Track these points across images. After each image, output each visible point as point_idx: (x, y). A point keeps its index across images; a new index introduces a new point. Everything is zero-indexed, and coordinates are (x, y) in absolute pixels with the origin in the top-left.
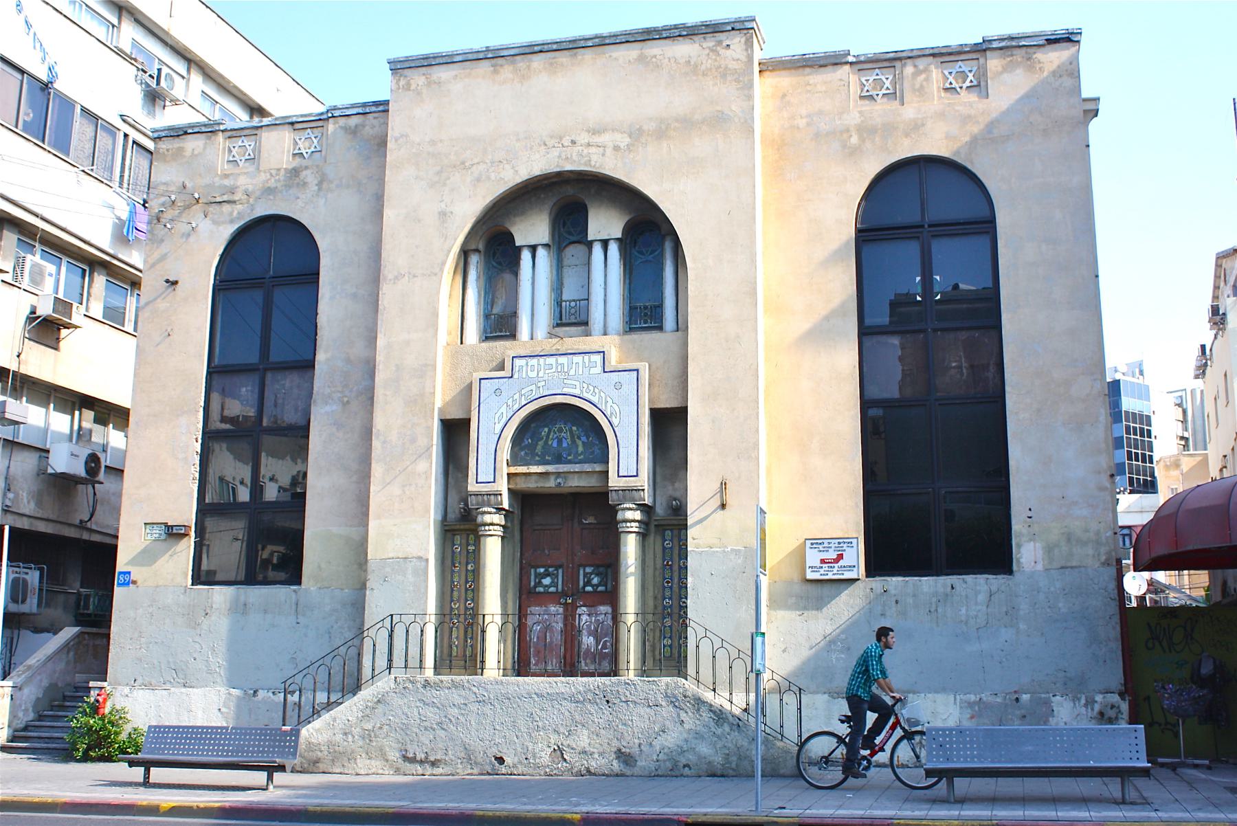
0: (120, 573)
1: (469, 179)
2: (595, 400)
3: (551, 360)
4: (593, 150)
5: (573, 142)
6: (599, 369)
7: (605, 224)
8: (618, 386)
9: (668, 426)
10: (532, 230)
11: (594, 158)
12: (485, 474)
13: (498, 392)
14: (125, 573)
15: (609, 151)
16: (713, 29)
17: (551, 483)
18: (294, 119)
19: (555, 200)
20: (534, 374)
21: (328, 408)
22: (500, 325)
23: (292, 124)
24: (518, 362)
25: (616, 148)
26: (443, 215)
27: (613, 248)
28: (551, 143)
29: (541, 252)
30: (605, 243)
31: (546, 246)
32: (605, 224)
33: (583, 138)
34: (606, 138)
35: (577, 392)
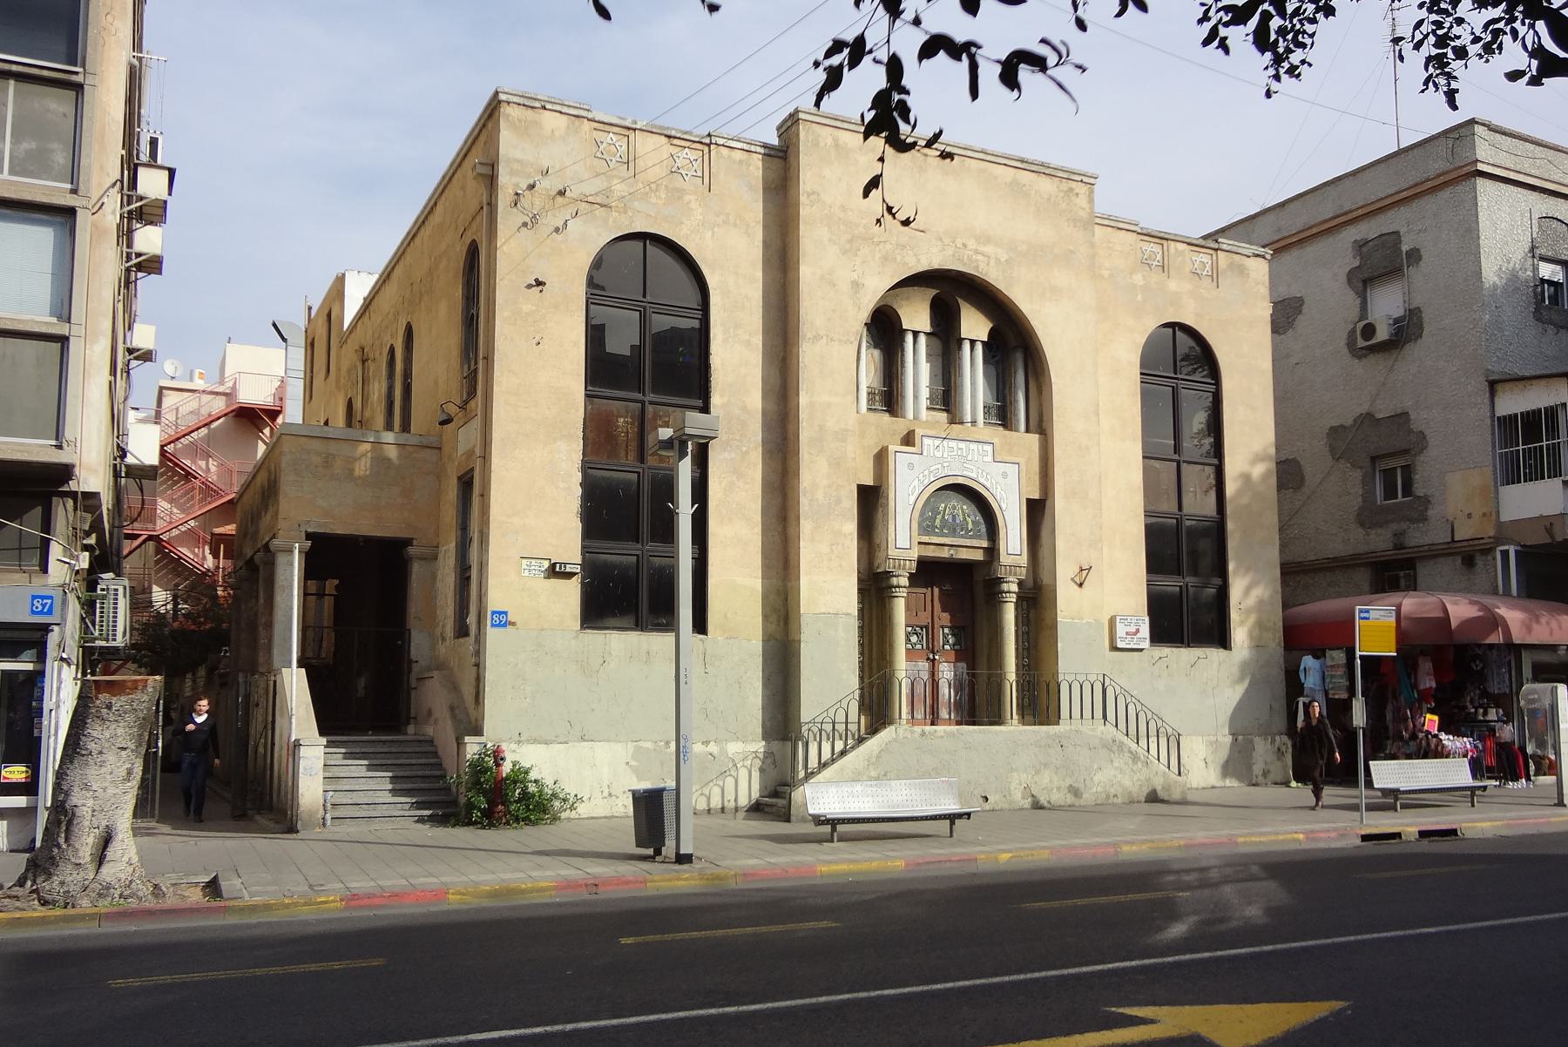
0: (494, 613)
1: (878, 255)
2: (988, 485)
3: (953, 444)
4: (980, 257)
5: (965, 245)
6: (990, 458)
7: (974, 325)
8: (1005, 475)
9: (1037, 511)
10: (916, 316)
11: (982, 266)
12: (903, 541)
13: (911, 466)
14: (500, 613)
15: (992, 262)
16: (1068, 175)
17: (945, 553)
18: (673, 133)
19: (934, 292)
20: (939, 454)
21: (726, 455)
22: (889, 398)
23: (669, 137)
24: (927, 441)
25: (998, 260)
26: (856, 285)
27: (979, 348)
28: (947, 241)
29: (922, 339)
30: (973, 342)
31: (927, 334)
32: (974, 325)
33: (972, 244)
34: (989, 249)
35: (973, 475)
